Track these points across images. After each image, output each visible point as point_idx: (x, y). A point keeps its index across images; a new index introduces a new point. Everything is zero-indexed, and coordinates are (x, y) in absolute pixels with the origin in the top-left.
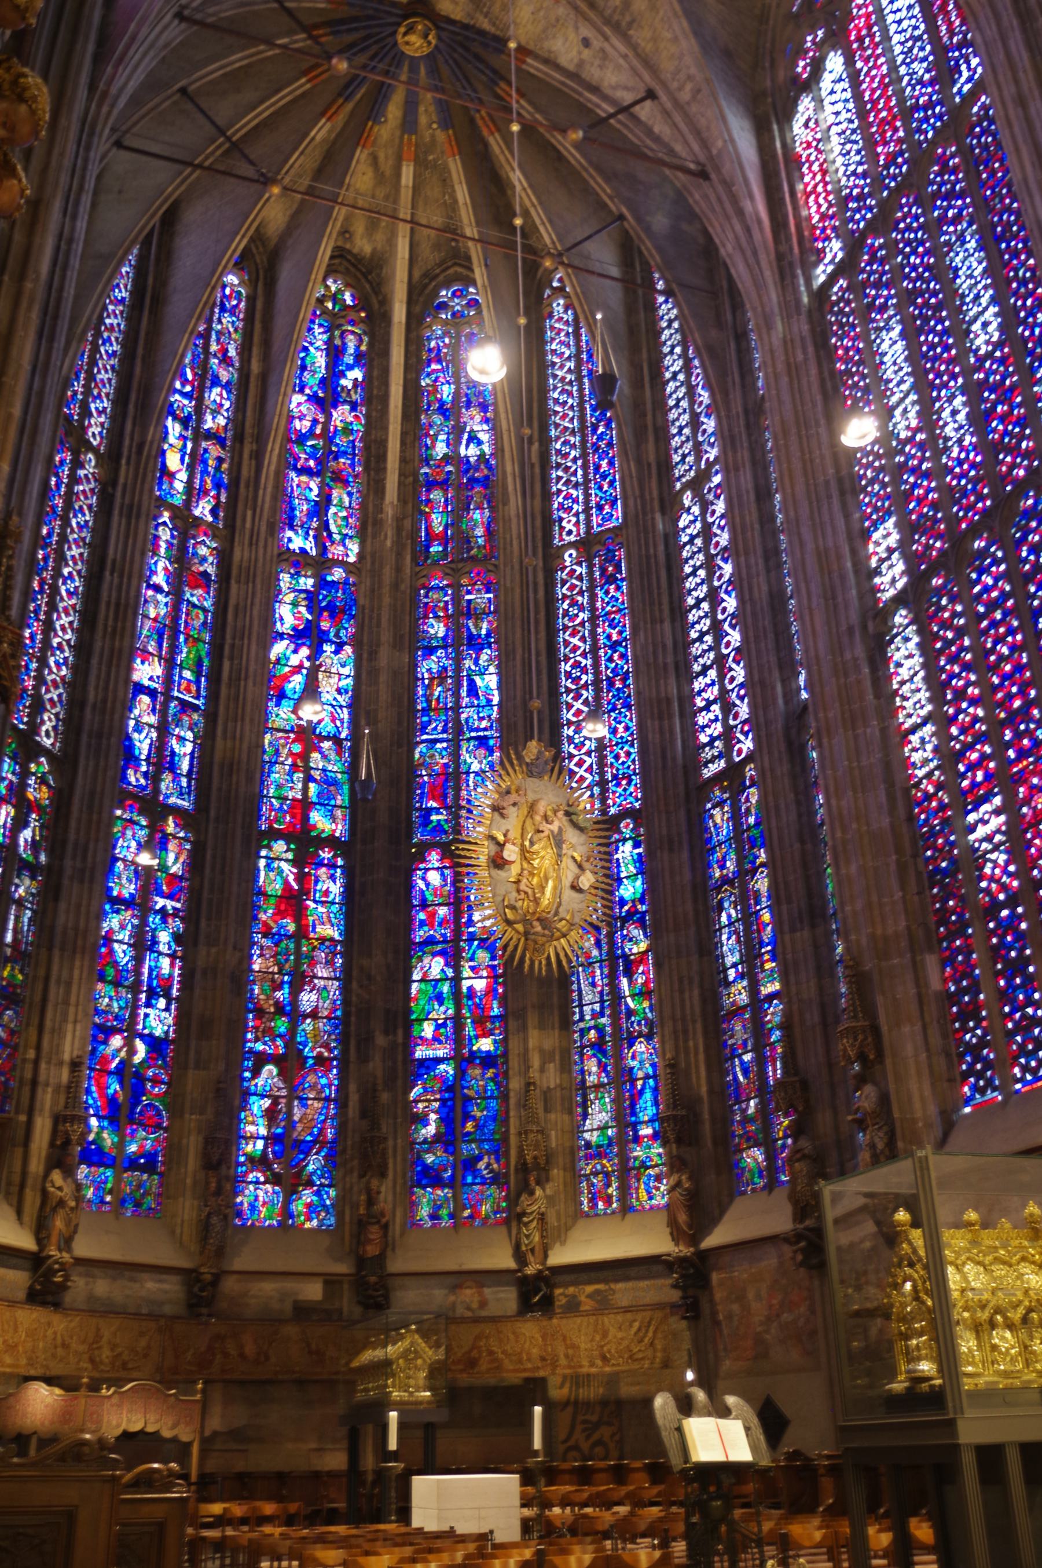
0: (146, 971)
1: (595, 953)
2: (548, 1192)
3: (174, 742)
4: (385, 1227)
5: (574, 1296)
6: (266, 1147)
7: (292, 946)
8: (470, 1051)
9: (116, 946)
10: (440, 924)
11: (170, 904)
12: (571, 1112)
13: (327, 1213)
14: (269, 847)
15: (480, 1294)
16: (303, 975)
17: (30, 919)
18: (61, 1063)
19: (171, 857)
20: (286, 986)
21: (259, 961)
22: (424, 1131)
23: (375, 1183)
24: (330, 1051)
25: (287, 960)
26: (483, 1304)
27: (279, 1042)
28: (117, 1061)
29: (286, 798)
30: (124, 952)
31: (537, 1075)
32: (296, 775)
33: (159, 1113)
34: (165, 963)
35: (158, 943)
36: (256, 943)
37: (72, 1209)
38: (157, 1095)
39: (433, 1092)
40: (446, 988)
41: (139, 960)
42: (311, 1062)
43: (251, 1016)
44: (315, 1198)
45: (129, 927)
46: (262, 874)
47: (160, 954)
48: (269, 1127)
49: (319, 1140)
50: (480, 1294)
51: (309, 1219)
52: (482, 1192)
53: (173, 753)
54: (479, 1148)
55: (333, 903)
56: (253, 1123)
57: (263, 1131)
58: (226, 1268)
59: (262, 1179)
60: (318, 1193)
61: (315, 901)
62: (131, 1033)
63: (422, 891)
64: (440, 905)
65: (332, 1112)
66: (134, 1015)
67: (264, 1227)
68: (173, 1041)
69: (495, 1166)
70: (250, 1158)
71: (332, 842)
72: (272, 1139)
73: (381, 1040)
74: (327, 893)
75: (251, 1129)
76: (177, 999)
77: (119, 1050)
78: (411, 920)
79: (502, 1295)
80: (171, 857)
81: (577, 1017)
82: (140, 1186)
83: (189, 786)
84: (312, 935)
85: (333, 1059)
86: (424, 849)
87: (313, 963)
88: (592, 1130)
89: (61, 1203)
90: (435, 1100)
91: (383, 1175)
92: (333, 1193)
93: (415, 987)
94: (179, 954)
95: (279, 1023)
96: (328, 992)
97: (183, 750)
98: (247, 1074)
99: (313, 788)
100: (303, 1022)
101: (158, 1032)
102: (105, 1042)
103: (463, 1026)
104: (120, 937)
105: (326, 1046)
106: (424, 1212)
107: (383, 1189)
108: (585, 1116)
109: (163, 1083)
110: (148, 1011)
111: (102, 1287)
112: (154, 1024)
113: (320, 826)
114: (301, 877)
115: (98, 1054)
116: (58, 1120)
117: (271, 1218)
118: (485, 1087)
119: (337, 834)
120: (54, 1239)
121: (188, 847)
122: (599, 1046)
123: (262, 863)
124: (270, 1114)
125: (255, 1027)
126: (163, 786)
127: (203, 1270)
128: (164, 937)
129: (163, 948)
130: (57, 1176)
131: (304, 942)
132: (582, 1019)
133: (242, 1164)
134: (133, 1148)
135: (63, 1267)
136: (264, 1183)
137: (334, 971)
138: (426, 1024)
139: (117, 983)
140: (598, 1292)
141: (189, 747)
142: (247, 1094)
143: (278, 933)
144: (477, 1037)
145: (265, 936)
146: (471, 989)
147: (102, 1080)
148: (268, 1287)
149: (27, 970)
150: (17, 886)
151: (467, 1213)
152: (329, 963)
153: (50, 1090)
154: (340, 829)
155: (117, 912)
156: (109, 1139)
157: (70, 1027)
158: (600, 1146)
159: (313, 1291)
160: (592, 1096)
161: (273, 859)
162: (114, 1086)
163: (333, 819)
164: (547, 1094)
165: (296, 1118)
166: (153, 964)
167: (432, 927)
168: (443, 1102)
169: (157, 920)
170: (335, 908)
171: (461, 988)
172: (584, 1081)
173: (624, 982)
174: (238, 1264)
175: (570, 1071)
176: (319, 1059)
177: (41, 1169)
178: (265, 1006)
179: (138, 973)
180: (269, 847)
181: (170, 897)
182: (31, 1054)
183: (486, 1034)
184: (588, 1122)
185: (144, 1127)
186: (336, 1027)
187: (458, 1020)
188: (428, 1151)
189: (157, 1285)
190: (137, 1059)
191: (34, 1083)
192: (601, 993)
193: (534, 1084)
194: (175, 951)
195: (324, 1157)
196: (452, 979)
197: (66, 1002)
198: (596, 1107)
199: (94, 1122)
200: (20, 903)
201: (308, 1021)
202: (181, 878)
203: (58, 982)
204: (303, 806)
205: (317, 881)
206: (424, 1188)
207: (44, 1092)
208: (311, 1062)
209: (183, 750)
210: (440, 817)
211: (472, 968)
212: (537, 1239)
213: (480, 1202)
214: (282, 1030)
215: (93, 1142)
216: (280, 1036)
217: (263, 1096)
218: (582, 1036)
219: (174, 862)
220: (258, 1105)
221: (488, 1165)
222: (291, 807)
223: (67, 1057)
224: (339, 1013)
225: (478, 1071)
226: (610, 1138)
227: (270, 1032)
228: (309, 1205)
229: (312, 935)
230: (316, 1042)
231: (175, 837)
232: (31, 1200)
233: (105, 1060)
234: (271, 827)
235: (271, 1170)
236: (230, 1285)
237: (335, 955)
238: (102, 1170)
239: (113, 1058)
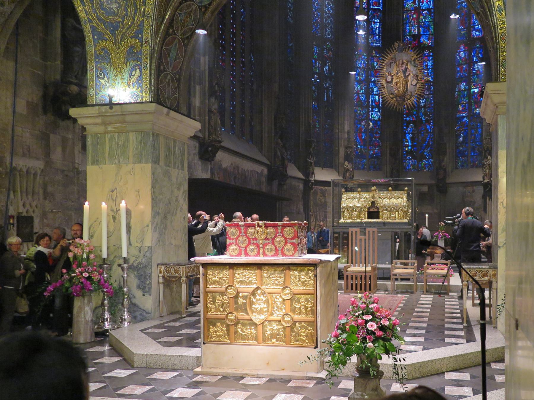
6: (411, 148)
24: (430, 118)
30: (363, 96)
33: (378, 142)
35: (374, 91)
37: (351, 171)
41: (368, 98)
48: (412, 143)
49: (428, 145)
51: (426, 168)
55: (429, 69)
57: (410, 144)
60: (428, 162)
62: (367, 119)
68: (381, 121)
74: (427, 66)
77: (364, 126)
101: (376, 118)
103: (472, 104)
112: (374, 116)
124: (412, 139)
130: (346, 163)
133: (405, 154)
139: (362, 106)
142: (405, 133)
153: (343, 140)
155: (360, 85)
157: (346, 122)
159: (425, 189)
162: (364, 136)
165: (420, 139)
167: (461, 72)
170: (430, 71)
171: (471, 91)
176: (427, 121)
177: (343, 161)
182: (337, 131)
208: (424, 121)
210: (464, 32)
214: (415, 113)
217: (409, 134)
220: (409, 136)
228: (425, 164)
232: (341, 170)
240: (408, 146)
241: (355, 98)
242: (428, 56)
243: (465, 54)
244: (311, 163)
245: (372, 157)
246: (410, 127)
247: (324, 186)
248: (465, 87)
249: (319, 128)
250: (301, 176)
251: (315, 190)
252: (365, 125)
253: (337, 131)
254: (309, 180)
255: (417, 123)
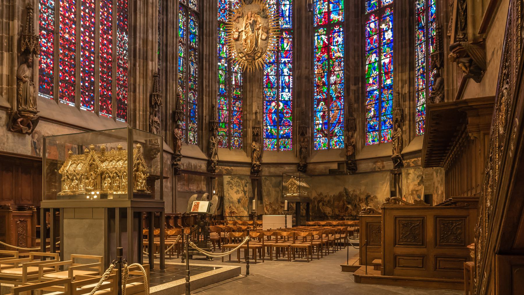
0: (281, 82)
1: (423, 38)
2: (404, 129)
3: (282, 6)
4: (354, 147)
5: (409, 163)
6: (322, 127)
7: (327, 63)
8: (384, 85)
9: (270, 77)
10: (375, 42)
11: (286, 60)
12: (413, 100)
13: (342, 143)
14: (318, 32)
15: (383, 164)
16: (331, 71)
17: (240, 76)
18: (253, 114)
19: (285, 45)
20: (326, 76)
21: (317, 70)
22: (370, 114)
23: (350, 133)
25: (326, 68)
26: (383, 167)
27: (324, 94)
28: (274, 109)
29: (322, 13)
31: (400, 90)
32: (325, 3)
33: (289, 122)
34: (287, 78)
35: (284, 73)
36: (315, 65)
38: (288, 117)
39: (373, 101)
40: (376, 65)
41: (278, 80)
42: (335, 98)
43: (315, 88)
44: (338, 140)
45: (274, 70)
46: (316, 41)
47: (285, 76)
48: (323, 121)
49: (339, 122)
50: (383, 164)
51: (336, 146)
52: (387, 132)
53: (282, 11)
54: (387, 118)
55: (340, 45)
56: (318, 120)
57: (321, 122)
58: (308, 162)
59: (321, 136)
60: (339, 139)
61: (334, 46)
62: (278, 100)
63: (368, 31)
64: (375, 35)
65: (342, 113)
66: (278, 95)
67: (323, 150)
68: (292, 101)
69: (391, 122)
70: (318, 131)
71: (339, 23)
72: (324, 124)
73: (353, 87)
75: (317, 122)
76: (292, 88)
77: (274, 106)
78: (365, 43)
79: (389, 164)
80: (285, 45)
81: (417, 65)
82: (285, 143)
83: (289, 19)
84: (333, 57)
85: (341, 97)
86: (370, 14)
87: (333, 68)
88: (420, 106)
89: (255, 150)
90: (373, 104)
91: (355, 130)
92: (343, 137)
93: (367, 66)
94: (291, 74)
95: (324, 88)
96: (339, 75)
97: (286, 8)
98: (315, 106)
99: (331, 5)
100: (332, 87)
101: (287, 99)
102: (270, 105)
103: (381, 77)
104: (271, 74)
105: (340, 93)
106: (370, 140)
107: (355, 135)
108: (418, 100)
109: (289, 113)
110: (282, 93)
111: (273, 170)
112: (285, 97)
113: (334, 19)
114: (329, 39)
115: (268, 109)
116: (253, 128)
117: (325, 147)
118: (388, 97)
119: (340, 20)
120: (254, 159)
121: (291, 40)
122: (422, 74)
123: (316, 38)
124: (323, 117)
125: (317, 91)
126: (280, 23)
127: (301, 163)
128: (286, 70)
129: (286, 74)
130: (254, 144)
131: (331, 60)
132: (418, 65)
133: (316, 133)
134: (282, 132)
135: (257, 165)
136: (322, 137)
137: (341, 67)
138: (370, 79)
139: (271, 88)
140: (415, 160)
141: (288, 6)
142: (316, 112)
143: (322, 60)
144: (386, 79)
145: (318, 61)
146: (384, 63)
147: (270, 115)
148: (322, 166)
149: (242, 90)
150: (234, 68)
151: (382, 139)
152: (339, 65)
154: (340, 18)
155: (269, 67)
156: (274, 131)
157: (254, 103)
158: (422, 111)
159: (335, 166)
160: (420, 93)
161: (319, 36)
162: (274, 116)
163: (339, 15)
164: (404, 96)
165: (331, 117)
166: (283, 79)
167: (372, 44)
168: (376, 104)
169: (283, 66)
172: (418, 88)
173: (431, 47)
174: (313, 160)
175: (414, 86)
176: (338, 98)
178: (320, 84)
179: (278, 83)
180: (318, 32)
181: (286, 57)
183: (388, 79)
184: (419, 103)
185: (285, 126)
186: (343, 86)
187: (380, 75)
188: (371, 121)
189: (289, 168)
190: (280, 108)
191: (247, 119)
192: (424, 54)
193: (399, 93)
194: (290, 74)
195: (340, 127)
196: (378, 61)
197: (252, 97)
198: (421, 97)
199: (269, 127)
200: (236, 72)
201: (333, 86)
202: (289, 51)
203: (250, 92)
204: (329, 13)
205: (334, 39)
206: (370, 132)
207: (250, 122)
208: (335, 98)
209: (286, 8)
211: (385, 55)
212: (397, 145)
213: (387, 135)
215: (270, 133)
216: (325, 93)
217: (320, 112)
218: (418, 72)
219: (287, 46)
221: (389, 122)
222: (324, 15)
223: (254, 111)
224: (343, 81)
225: (386, 91)
226: (425, 107)
227: (321, 92)
228: (336, 142)
229: (333, 57)
230: (336, 92)
231: (286, 38)
233: (271, 110)
234: (318, 24)
235: (324, 132)
236: (310, 167)
237: (341, 62)
238: (273, 139)
239: (273, 109)
240: (318, 124)
241: (264, 80)
242: (338, 32)
243: (375, 24)
244: (214, 144)
245: (282, 137)
246: (320, 105)
247: (230, 166)
248: (375, 59)
249: (226, 110)
250: (204, 156)
251: (220, 170)
252: (275, 106)
253: (245, 113)
254: (211, 160)
255: (328, 101)
